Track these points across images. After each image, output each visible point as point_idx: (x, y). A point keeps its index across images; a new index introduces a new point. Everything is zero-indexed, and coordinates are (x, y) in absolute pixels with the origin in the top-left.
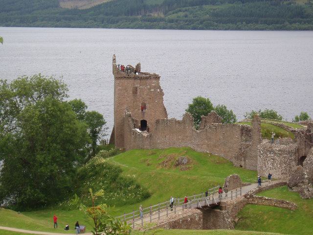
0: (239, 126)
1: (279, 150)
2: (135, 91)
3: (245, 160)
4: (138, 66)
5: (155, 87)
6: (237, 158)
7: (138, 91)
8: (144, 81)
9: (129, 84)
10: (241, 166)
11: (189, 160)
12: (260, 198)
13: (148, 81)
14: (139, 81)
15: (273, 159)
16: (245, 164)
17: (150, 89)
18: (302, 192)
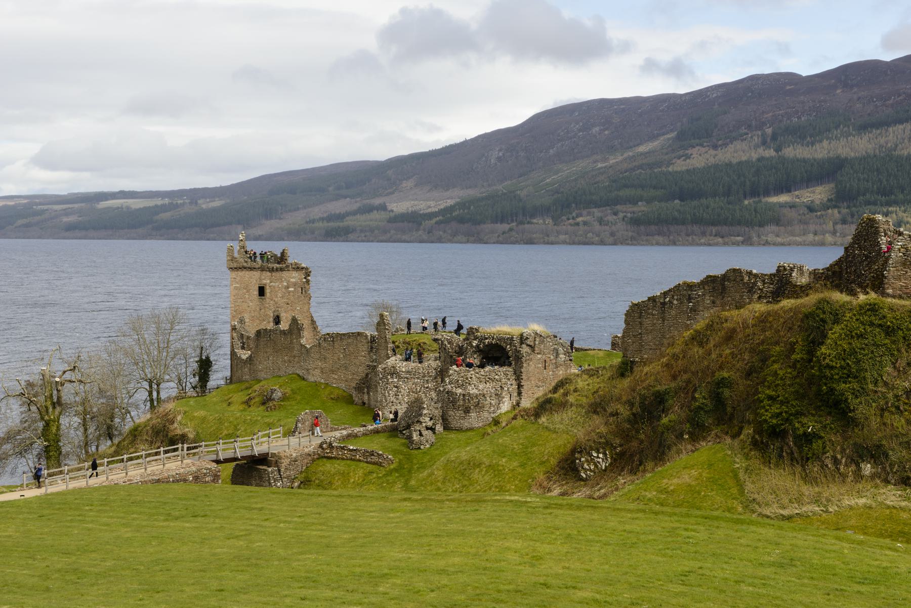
0: (366, 336)
1: (408, 372)
2: (262, 291)
3: (368, 393)
4: (283, 253)
5: (295, 285)
6: (359, 389)
7: (268, 291)
8: (278, 274)
9: (254, 279)
10: (364, 404)
11: (284, 394)
12: (343, 448)
13: (285, 274)
14: (269, 274)
15: (396, 387)
16: (369, 399)
17: (288, 287)
18: (410, 438)
